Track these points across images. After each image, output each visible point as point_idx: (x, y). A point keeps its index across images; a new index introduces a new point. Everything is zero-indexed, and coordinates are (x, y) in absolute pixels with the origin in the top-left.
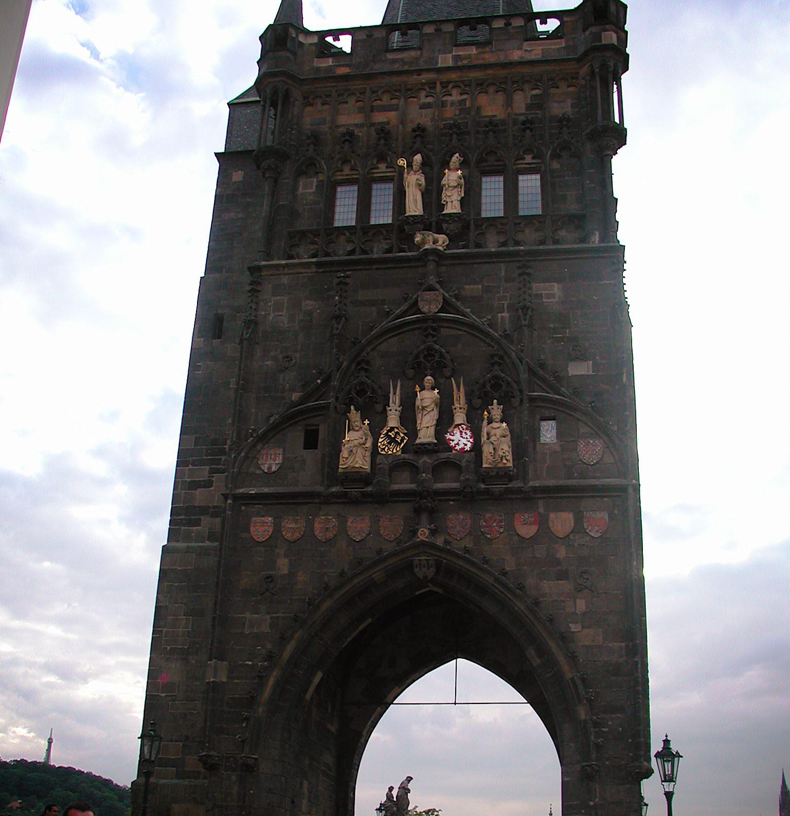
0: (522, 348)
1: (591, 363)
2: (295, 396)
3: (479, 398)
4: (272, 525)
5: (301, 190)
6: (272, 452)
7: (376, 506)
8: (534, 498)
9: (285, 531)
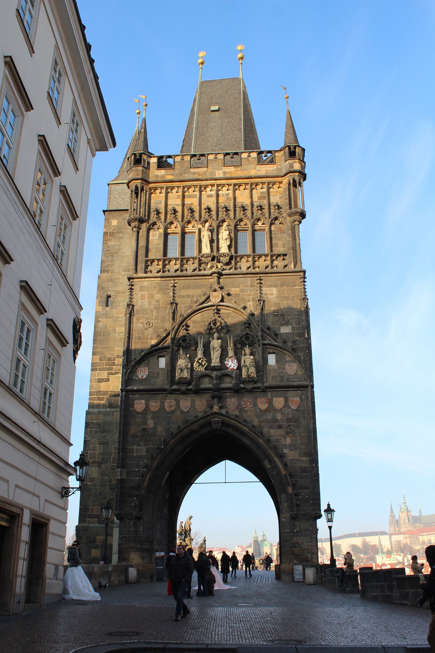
1: (291, 327)
2: (154, 342)
3: (240, 344)
5: (151, 238)
6: (143, 369)
7: (193, 395)
8: (266, 391)
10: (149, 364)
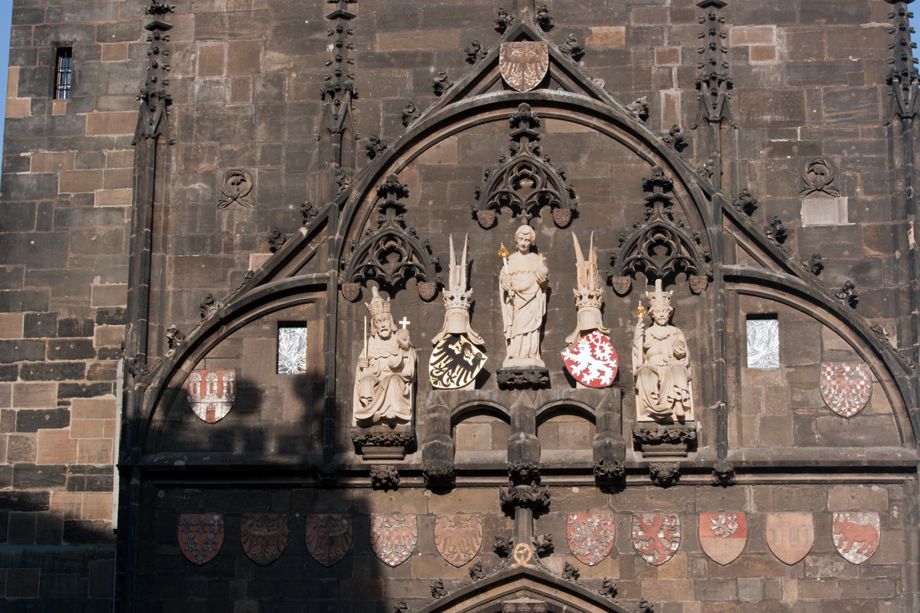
0: (710, 168)
1: (845, 200)
2: (258, 260)
4: (222, 530)
7: (428, 493)
9: (248, 543)
10: (238, 357)
